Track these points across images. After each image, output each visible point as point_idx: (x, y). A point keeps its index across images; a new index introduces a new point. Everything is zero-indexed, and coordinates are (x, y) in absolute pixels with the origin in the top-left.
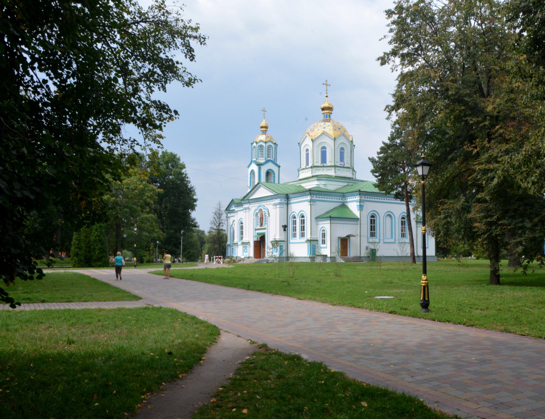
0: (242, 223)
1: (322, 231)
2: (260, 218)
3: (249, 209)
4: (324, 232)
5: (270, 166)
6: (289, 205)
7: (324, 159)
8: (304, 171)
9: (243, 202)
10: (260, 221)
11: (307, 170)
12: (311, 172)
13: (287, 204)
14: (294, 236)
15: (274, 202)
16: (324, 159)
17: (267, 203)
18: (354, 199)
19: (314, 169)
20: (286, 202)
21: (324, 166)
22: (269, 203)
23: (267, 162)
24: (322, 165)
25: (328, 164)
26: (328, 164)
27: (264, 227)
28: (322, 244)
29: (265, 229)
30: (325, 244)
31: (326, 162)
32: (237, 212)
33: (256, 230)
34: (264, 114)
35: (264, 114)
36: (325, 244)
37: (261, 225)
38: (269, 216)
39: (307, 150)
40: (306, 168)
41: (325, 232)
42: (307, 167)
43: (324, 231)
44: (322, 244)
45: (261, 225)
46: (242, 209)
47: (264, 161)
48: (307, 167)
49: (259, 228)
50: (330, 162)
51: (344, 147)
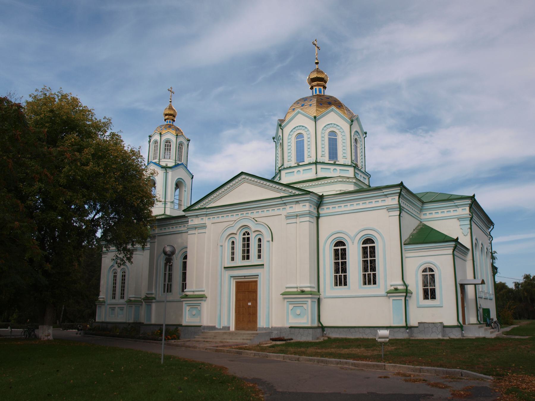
1: (425, 271)
3: (204, 226)
4: (428, 273)
5: (180, 173)
6: (321, 220)
7: (333, 153)
8: (295, 170)
9: (187, 214)
11: (301, 169)
13: (318, 218)
15: (292, 210)
16: (333, 153)
17: (266, 213)
18: (452, 213)
19: (319, 167)
20: (315, 211)
21: (334, 164)
22: (271, 213)
24: (332, 162)
25: (341, 161)
26: (341, 161)
28: (426, 297)
30: (433, 297)
34: (171, 96)
35: (171, 96)
36: (433, 297)
38: (272, 241)
39: (300, 135)
40: (299, 166)
41: (436, 273)
42: (301, 164)
43: (431, 270)
44: (426, 297)
47: (173, 164)
50: (344, 157)
51: (358, 139)
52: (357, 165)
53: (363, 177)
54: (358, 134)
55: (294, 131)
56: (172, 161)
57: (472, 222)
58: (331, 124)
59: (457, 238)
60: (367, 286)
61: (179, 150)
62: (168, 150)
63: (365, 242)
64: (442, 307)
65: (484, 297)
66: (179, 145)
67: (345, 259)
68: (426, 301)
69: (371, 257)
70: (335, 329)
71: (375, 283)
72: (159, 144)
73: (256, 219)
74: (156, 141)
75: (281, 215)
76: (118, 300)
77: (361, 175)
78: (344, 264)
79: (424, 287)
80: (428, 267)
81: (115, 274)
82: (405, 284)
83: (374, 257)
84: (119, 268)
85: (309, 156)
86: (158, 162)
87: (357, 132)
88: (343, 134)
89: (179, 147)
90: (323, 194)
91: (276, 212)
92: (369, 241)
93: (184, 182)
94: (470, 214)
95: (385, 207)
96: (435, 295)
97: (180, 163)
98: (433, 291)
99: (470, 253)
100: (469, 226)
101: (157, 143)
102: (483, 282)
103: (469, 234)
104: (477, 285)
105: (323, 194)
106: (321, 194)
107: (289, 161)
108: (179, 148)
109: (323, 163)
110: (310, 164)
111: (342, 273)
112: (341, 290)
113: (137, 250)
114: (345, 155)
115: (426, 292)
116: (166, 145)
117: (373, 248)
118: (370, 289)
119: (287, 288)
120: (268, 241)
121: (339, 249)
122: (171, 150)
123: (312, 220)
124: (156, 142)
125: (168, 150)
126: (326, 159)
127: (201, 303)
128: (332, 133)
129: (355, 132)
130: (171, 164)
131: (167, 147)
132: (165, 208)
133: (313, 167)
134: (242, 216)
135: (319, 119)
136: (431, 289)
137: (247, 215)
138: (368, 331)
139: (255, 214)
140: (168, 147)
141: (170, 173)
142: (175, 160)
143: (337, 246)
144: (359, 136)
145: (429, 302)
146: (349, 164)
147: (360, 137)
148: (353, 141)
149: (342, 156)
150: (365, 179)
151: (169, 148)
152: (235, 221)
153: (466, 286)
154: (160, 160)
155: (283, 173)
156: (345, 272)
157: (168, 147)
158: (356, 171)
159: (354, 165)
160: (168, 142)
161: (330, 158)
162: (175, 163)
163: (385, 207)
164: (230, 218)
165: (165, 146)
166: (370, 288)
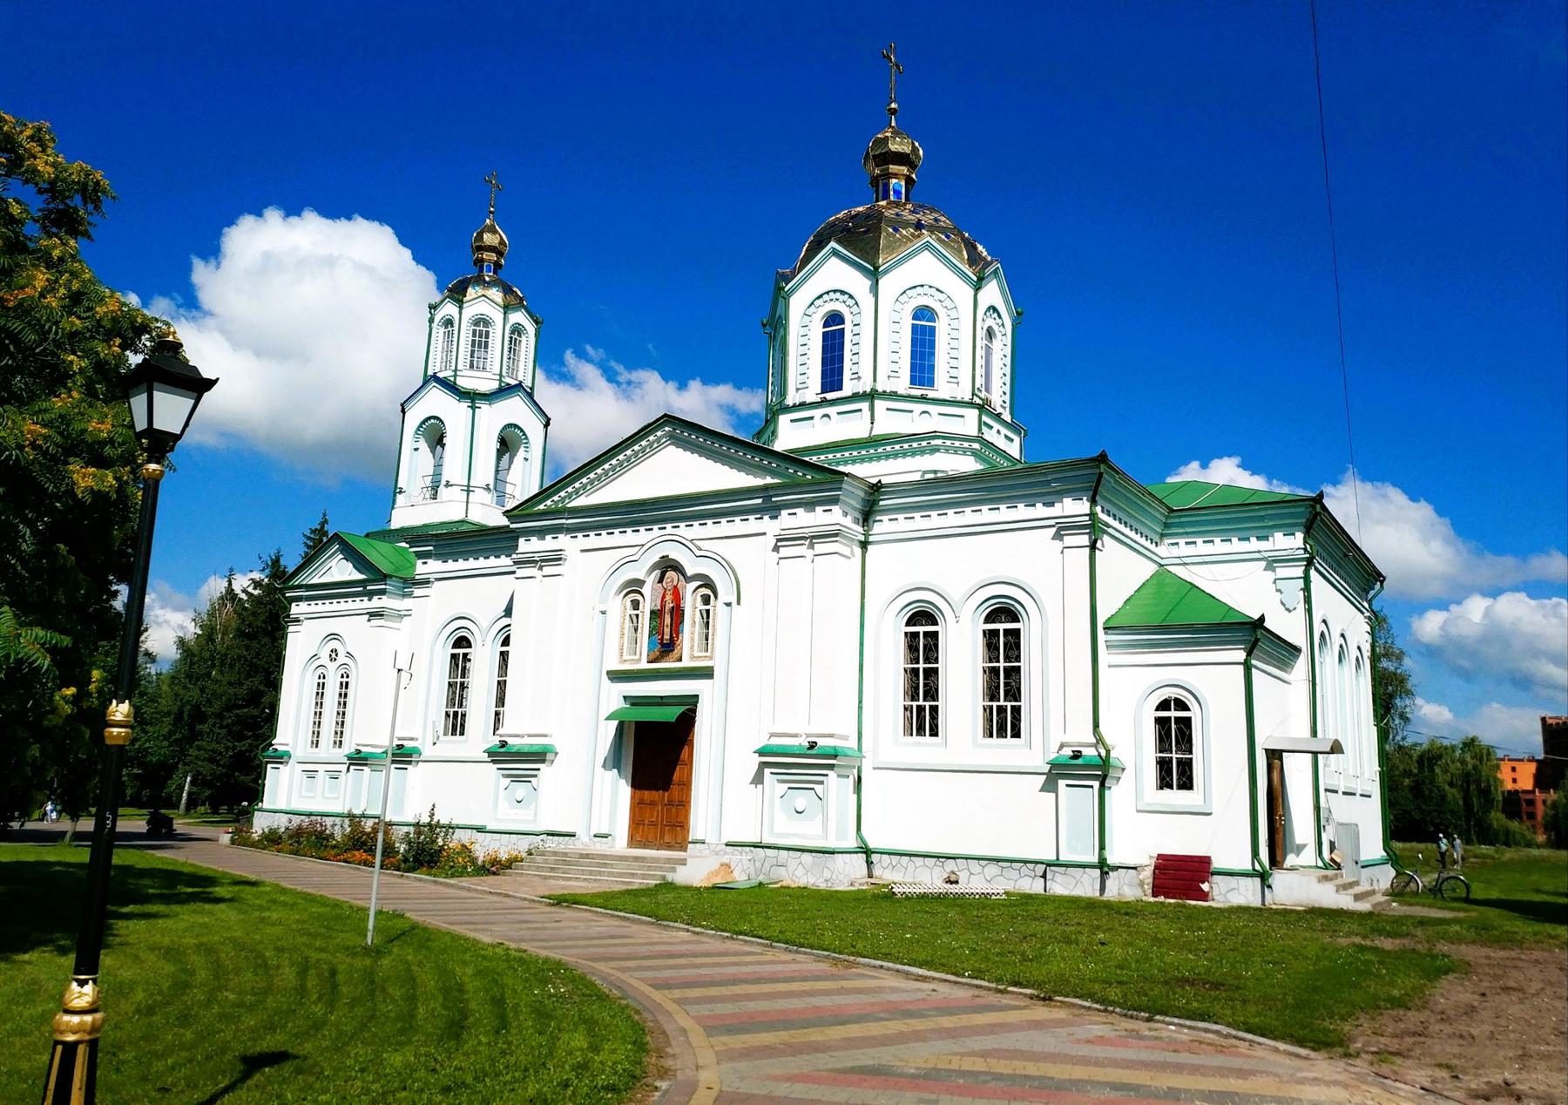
0: (462, 642)
1: (1164, 705)
2: (656, 615)
3: (556, 558)
4: (1173, 714)
7: (922, 370)
8: (817, 413)
10: (655, 630)
11: (832, 410)
12: (866, 413)
14: (924, 721)
16: (922, 370)
19: (880, 405)
21: (923, 399)
23: (504, 391)
24: (918, 392)
26: (942, 389)
27: (686, 663)
28: (1164, 783)
29: (707, 673)
30: (1186, 784)
31: (930, 383)
32: (425, 582)
33: (617, 676)
36: (1186, 784)
37: (666, 647)
38: (739, 603)
39: (834, 318)
40: (823, 403)
41: (1194, 714)
43: (1182, 706)
44: (1164, 783)
45: (666, 647)
46: (504, 561)
47: (494, 385)
48: (830, 396)
49: (644, 665)
51: (996, 328)
52: (987, 402)
53: (1006, 436)
54: (995, 315)
55: (818, 303)
56: (489, 375)
57: (1313, 572)
58: (922, 286)
59: (1262, 619)
60: (995, 740)
61: (510, 348)
62: (480, 347)
63: (989, 619)
64: (1210, 814)
65: (1342, 789)
66: (513, 332)
67: (936, 661)
68: (1167, 791)
69: (1007, 659)
70: (903, 857)
71: (1016, 734)
72: (456, 328)
73: (698, 543)
74: (449, 319)
75: (764, 534)
76: (327, 750)
77: (998, 432)
78: (932, 674)
79: (1160, 752)
80: (1173, 696)
81: (321, 681)
82: (1100, 740)
83: (1018, 659)
84: (334, 663)
85: (856, 376)
86: (452, 379)
87: (995, 310)
88: (953, 314)
89: (511, 338)
90: (880, 481)
91: (753, 524)
92: (1003, 612)
93: (524, 434)
94: (1305, 549)
95: (1052, 522)
96: (1190, 778)
97: (513, 382)
98: (1186, 767)
99: (1302, 663)
100: (1301, 583)
101: (452, 326)
102: (1336, 748)
103: (1301, 607)
104: (1320, 756)
105: (880, 481)
106: (874, 481)
107: (800, 386)
108: (511, 341)
109: (893, 396)
110: (856, 397)
111: (924, 700)
112: (923, 749)
113: (382, 615)
114: (954, 372)
115: (1164, 766)
116: (474, 331)
117: (1016, 634)
118: (1004, 751)
119: (772, 735)
120: (728, 605)
121: (918, 633)
122: (490, 345)
123: (846, 550)
124: (448, 322)
125: (480, 347)
126: (902, 385)
127: (539, 769)
128: (923, 313)
129: (989, 309)
130: (489, 386)
131: (477, 339)
132: (467, 502)
133: (865, 406)
134: (663, 532)
135: (886, 271)
136: (1179, 761)
137: (675, 531)
138: (993, 869)
139: (695, 531)
140: (481, 336)
141: (484, 409)
142: (501, 375)
143: (915, 625)
144: (1000, 321)
145: (1175, 797)
146: (967, 399)
147: (1003, 324)
148: (981, 334)
149: (948, 375)
150: (1012, 440)
151: (477, 339)
152: (643, 545)
153: (1284, 754)
154: (458, 373)
155: (784, 420)
156: (935, 697)
157: (481, 336)
158: (984, 418)
159: (981, 402)
160: (482, 321)
161: (913, 381)
162: (500, 381)
163: (1052, 522)
164: (630, 537)
165: (474, 335)
166: (1002, 746)
